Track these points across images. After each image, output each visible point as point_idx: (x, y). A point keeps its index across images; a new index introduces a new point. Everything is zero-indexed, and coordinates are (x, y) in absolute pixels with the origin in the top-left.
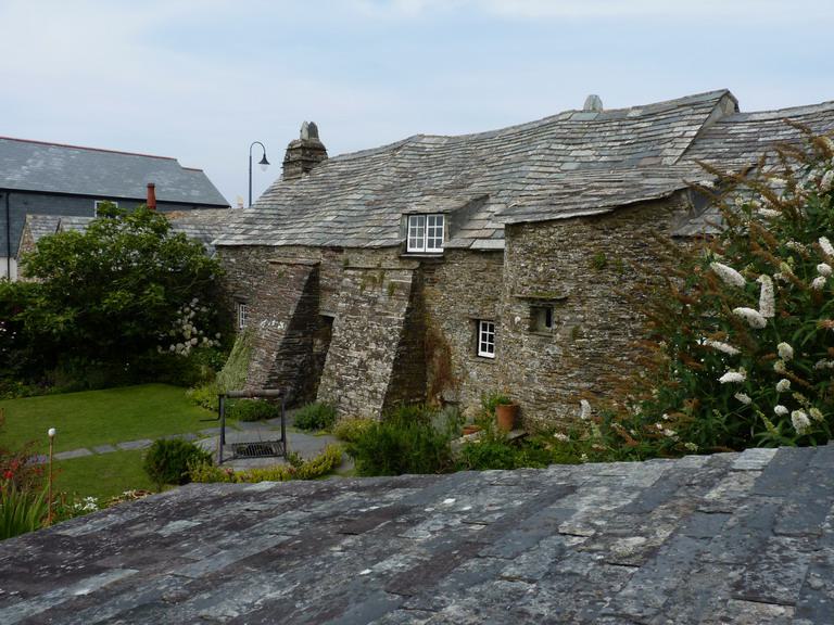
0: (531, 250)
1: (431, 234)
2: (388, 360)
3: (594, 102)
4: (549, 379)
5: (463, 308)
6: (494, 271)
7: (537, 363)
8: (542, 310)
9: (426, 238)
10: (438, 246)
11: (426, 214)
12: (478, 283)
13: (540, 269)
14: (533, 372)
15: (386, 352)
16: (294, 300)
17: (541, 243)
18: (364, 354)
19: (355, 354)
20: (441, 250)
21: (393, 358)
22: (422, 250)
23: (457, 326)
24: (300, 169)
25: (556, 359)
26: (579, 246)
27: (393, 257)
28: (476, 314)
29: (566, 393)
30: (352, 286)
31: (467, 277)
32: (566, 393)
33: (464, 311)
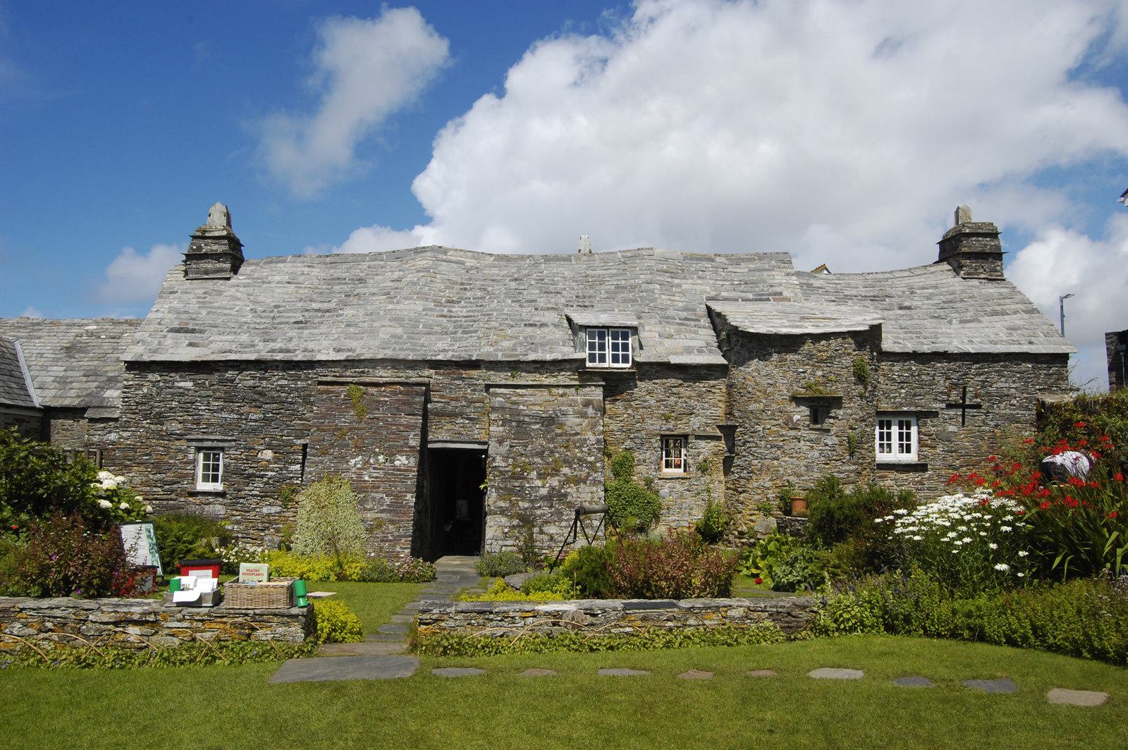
1: (615, 347)
2: (595, 483)
4: (827, 466)
5: (656, 425)
7: (817, 454)
8: (821, 408)
9: (609, 353)
10: (625, 359)
11: (608, 328)
12: (672, 398)
13: (819, 373)
14: (813, 462)
16: (410, 427)
17: (820, 351)
18: (554, 482)
19: (538, 483)
20: (629, 365)
22: (606, 365)
24: (228, 266)
26: (849, 354)
28: (668, 429)
29: (842, 476)
30: (508, 405)
32: (842, 476)
33: (654, 427)
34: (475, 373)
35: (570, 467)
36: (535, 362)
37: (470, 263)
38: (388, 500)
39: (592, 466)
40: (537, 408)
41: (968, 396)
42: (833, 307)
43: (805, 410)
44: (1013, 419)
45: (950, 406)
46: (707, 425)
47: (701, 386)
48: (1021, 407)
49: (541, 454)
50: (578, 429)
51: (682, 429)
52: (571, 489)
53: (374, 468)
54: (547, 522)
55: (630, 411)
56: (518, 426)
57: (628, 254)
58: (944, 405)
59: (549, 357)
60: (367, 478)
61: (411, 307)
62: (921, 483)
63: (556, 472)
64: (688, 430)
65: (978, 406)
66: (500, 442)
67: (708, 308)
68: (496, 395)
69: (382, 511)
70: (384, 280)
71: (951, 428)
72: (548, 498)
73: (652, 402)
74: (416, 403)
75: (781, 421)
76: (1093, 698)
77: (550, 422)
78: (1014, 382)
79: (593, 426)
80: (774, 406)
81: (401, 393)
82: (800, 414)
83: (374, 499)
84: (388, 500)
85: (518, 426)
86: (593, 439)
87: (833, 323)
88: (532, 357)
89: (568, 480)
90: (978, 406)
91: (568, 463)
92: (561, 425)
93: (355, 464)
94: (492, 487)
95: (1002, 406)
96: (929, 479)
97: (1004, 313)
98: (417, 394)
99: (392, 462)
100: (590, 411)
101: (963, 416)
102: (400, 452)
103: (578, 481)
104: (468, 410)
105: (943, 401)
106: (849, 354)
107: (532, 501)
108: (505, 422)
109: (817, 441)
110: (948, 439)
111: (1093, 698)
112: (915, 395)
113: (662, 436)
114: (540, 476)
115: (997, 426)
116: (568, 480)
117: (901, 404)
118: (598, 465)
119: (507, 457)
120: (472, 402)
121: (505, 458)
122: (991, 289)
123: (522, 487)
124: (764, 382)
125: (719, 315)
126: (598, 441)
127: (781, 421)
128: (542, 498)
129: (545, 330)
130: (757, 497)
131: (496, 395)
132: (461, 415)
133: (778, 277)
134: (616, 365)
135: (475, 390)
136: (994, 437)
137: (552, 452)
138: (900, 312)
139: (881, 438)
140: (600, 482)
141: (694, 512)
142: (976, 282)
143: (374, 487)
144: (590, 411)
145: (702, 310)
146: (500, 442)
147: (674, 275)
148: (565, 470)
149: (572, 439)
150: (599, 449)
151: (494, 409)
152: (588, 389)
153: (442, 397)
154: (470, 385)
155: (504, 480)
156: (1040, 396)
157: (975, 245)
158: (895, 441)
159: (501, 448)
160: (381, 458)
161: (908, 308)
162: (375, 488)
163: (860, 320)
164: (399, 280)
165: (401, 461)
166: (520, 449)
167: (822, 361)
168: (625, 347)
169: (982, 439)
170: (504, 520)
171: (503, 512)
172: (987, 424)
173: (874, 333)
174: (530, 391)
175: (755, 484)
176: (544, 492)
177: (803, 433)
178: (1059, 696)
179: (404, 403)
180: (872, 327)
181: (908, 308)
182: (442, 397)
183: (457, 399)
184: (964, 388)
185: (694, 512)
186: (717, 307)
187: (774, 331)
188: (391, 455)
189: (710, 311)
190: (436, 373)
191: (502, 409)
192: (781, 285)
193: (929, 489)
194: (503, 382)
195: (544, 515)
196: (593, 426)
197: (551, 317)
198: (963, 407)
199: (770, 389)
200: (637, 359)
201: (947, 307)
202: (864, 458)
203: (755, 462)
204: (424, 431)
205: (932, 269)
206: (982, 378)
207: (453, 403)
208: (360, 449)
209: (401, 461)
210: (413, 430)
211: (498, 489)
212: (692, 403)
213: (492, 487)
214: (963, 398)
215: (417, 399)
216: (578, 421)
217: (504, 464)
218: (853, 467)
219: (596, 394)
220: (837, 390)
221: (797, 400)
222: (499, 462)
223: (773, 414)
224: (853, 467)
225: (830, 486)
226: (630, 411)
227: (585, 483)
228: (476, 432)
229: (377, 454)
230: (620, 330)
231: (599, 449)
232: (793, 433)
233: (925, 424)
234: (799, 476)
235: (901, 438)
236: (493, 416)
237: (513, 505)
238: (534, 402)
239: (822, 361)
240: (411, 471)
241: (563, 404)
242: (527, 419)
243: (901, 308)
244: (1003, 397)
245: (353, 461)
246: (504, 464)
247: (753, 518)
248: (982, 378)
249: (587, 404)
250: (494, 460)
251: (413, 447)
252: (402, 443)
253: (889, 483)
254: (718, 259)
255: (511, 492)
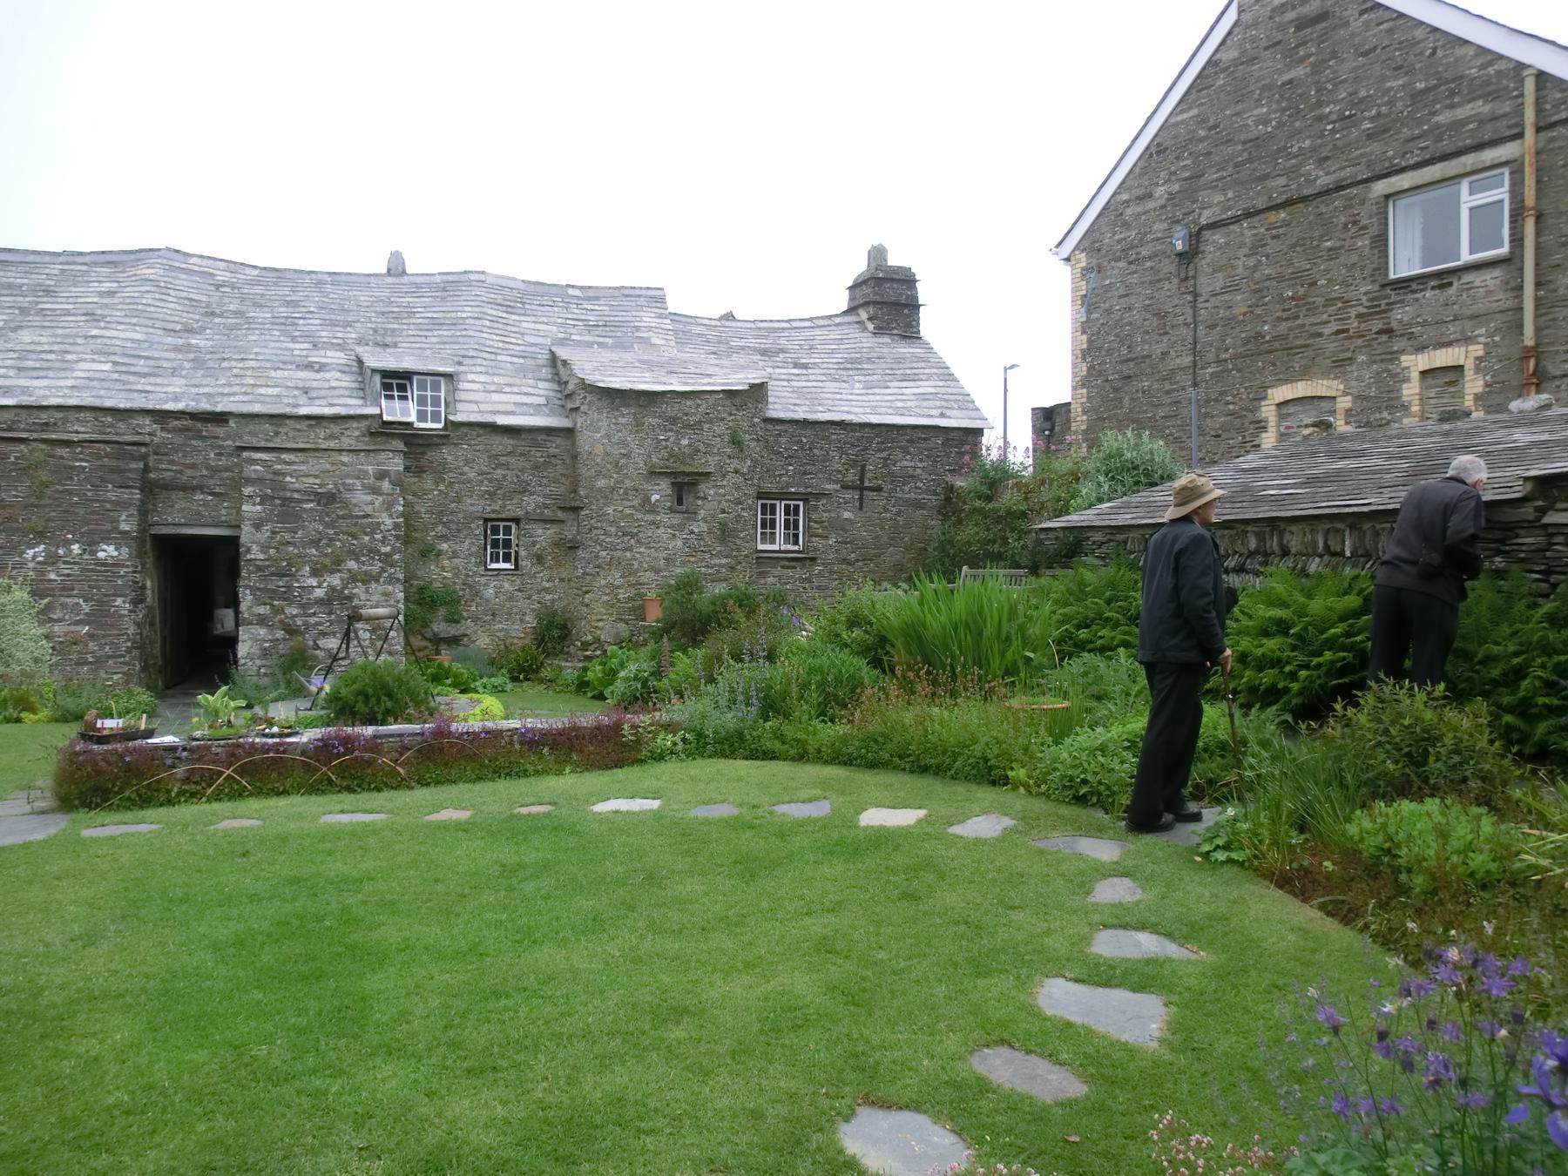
0: (674, 421)
2: (392, 580)
3: (396, 268)
5: (475, 505)
6: (522, 455)
7: (680, 543)
8: (685, 485)
10: (436, 417)
13: (685, 442)
15: (383, 570)
16: (121, 505)
18: (335, 580)
20: (441, 426)
21: (401, 576)
23: (459, 531)
25: (700, 537)
26: (723, 419)
27: (357, 433)
28: (494, 511)
30: (270, 476)
31: (482, 463)
33: (474, 509)
34: (220, 431)
35: (357, 560)
36: (308, 417)
37: (222, 276)
38: (86, 608)
39: (387, 559)
40: (311, 480)
41: (868, 475)
42: (712, 359)
43: (665, 485)
44: (918, 505)
45: (845, 487)
46: (546, 506)
47: (538, 456)
48: (927, 491)
49: (315, 543)
50: (369, 509)
51: (512, 510)
52: (359, 590)
53: (66, 563)
54: (324, 634)
55: (442, 487)
56: (284, 507)
57: (450, 278)
58: (838, 487)
59: (327, 411)
60: (53, 576)
61: (125, 334)
62: (809, 580)
63: (336, 565)
64: (520, 513)
65: (878, 489)
66: (258, 526)
67: (552, 353)
68: (254, 462)
69: (77, 623)
70: (88, 295)
71: (847, 515)
72: (325, 603)
73: (472, 475)
74: (130, 471)
75: (635, 502)
76: (905, 817)
77: (328, 499)
78: (921, 460)
79: (388, 507)
80: (628, 483)
81: (107, 455)
82: (660, 493)
83: (64, 606)
84: (86, 608)
85: (284, 507)
86: (389, 522)
87: (706, 380)
88: (303, 411)
89: (353, 578)
90: (878, 489)
91: (355, 555)
92: (346, 505)
93: (34, 557)
94: (247, 587)
95: (907, 488)
96: (820, 574)
97: (914, 379)
98: (133, 458)
99: (93, 553)
100: (386, 485)
101: (861, 499)
102: (107, 540)
103: (367, 579)
104: (211, 482)
105: (836, 482)
106: (723, 419)
107: (303, 606)
108: (264, 499)
109: (681, 527)
110: (841, 527)
111: (905, 817)
112: (805, 473)
113: (486, 520)
114: (315, 573)
115: (899, 513)
116: (353, 578)
117: (788, 485)
118: (397, 557)
119: (269, 547)
120: (215, 470)
121: (265, 548)
122: (904, 349)
123: (289, 588)
124: (616, 451)
125: (565, 363)
126: (396, 526)
127: (635, 502)
128: (319, 602)
129: (327, 375)
130: (605, 598)
131: (254, 462)
132: (201, 488)
133: (648, 318)
134: (423, 425)
135: (221, 454)
136: (896, 526)
137: (331, 540)
138: (796, 371)
139: (764, 526)
140: (398, 580)
141: (527, 618)
142: (887, 340)
143: (63, 589)
144: (386, 485)
145: (544, 356)
146: (258, 526)
147: (510, 310)
148: (352, 565)
149: (362, 524)
150: (397, 537)
151: (249, 481)
152: (382, 456)
153: (172, 462)
154: (213, 447)
155: (264, 578)
156: (949, 478)
157: (890, 293)
158: (780, 530)
159: (259, 535)
160: (76, 548)
161: (805, 366)
162: (66, 590)
163: (739, 380)
164: (110, 294)
165: (107, 551)
166: (287, 536)
167: (690, 426)
168: (436, 401)
169: (882, 528)
170: (262, 631)
171: (262, 621)
172: (886, 510)
173: (758, 391)
174: (300, 457)
175: (603, 582)
176: (319, 593)
177: (663, 517)
178: (874, 818)
179: (112, 471)
180: (753, 386)
181: (805, 366)
182: (172, 462)
183: (193, 466)
184: (863, 467)
185: (527, 618)
186: (562, 353)
187: (627, 386)
188: (91, 544)
189: (554, 360)
190: (162, 429)
191: (259, 481)
192: (650, 329)
193: (819, 588)
194: (263, 444)
195: (320, 624)
196: (388, 507)
197: (335, 357)
198: (862, 489)
199: (623, 461)
200: (451, 418)
201: (852, 365)
202: (738, 550)
203: (603, 553)
204: (143, 513)
205: (838, 320)
206: (884, 454)
207: (189, 472)
208: (41, 536)
209: (107, 551)
210: (126, 509)
211: (253, 590)
212: (526, 477)
213: (247, 587)
214: (862, 479)
215: (133, 465)
216: (369, 498)
217: (262, 556)
218: (724, 561)
219: (396, 464)
220: (711, 464)
221: (653, 474)
222: (255, 553)
223: (626, 493)
224: (724, 561)
225: (689, 585)
226: (442, 487)
227: (377, 581)
228: (224, 512)
229: (68, 543)
230: (429, 378)
231: (397, 537)
232: (650, 517)
233: (816, 508)
234: (657, 571)
235: (787, 527)
236: (247, 491)
237: (278, 611)
238: (303, 475)
239: (690, 426)
240: (123, 566)
241: (348, 476)
242: (296, 496)
243: (796, 366)
244: (909, 477)
245: (31, 553)
246: (262, 556)
247: (600, 624)
248: (884, 454)
249: (381, 475)
250: (248, 550)
251: (127, 532)
252: (108, 526)
253: (770, 580)
254: (571, 292)
255: (273, 594)
